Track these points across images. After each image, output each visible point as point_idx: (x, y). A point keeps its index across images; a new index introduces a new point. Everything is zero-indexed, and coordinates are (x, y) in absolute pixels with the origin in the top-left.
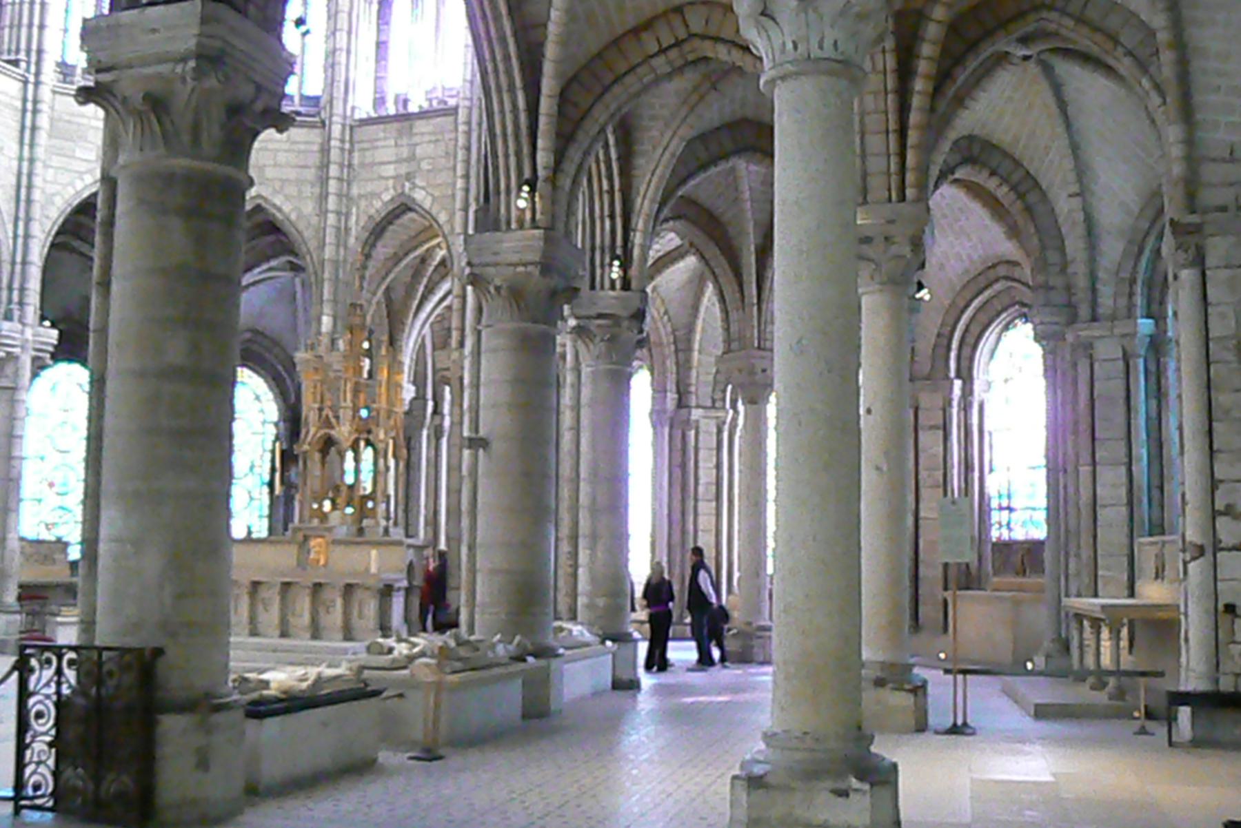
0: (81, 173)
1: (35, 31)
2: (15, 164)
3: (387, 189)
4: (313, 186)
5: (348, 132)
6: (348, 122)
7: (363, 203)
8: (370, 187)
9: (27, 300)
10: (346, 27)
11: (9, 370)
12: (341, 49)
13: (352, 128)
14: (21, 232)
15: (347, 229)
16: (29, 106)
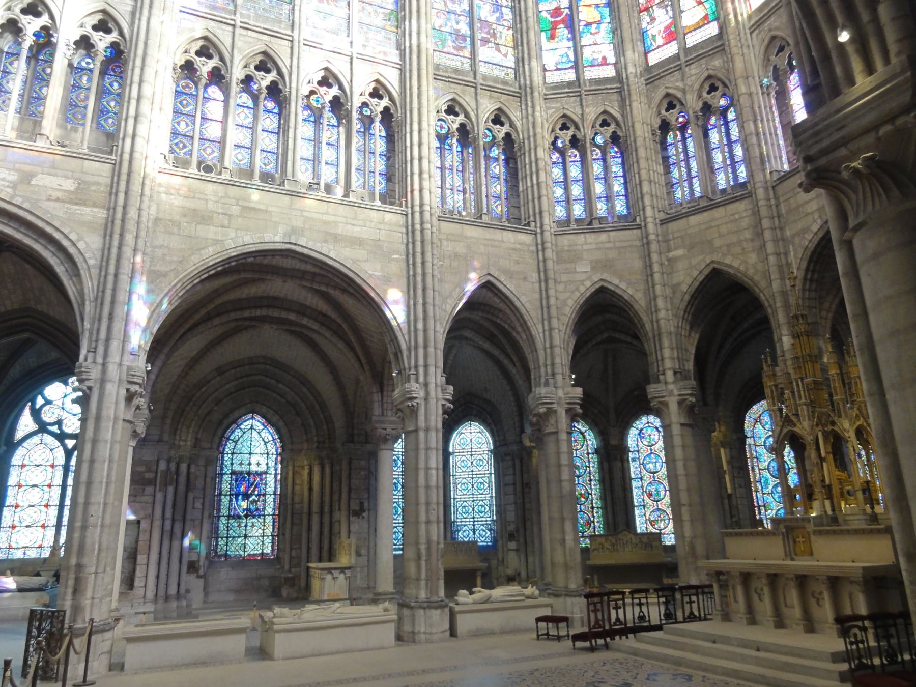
0: (582, 282)
1: (536, 201)
2: (537, 286)
3: (815, 221)
4: (752, 240)
5: (771, 193)
6: (769, 184)
7: (797, 240)
8: (799, 226)
9: (556, 371)
10: (751, 117)
11: (552, 421)
12: (751, 134)
13: (773, 187)
14: (546, 328)
15: (789, 265)
16: (540, 247)
